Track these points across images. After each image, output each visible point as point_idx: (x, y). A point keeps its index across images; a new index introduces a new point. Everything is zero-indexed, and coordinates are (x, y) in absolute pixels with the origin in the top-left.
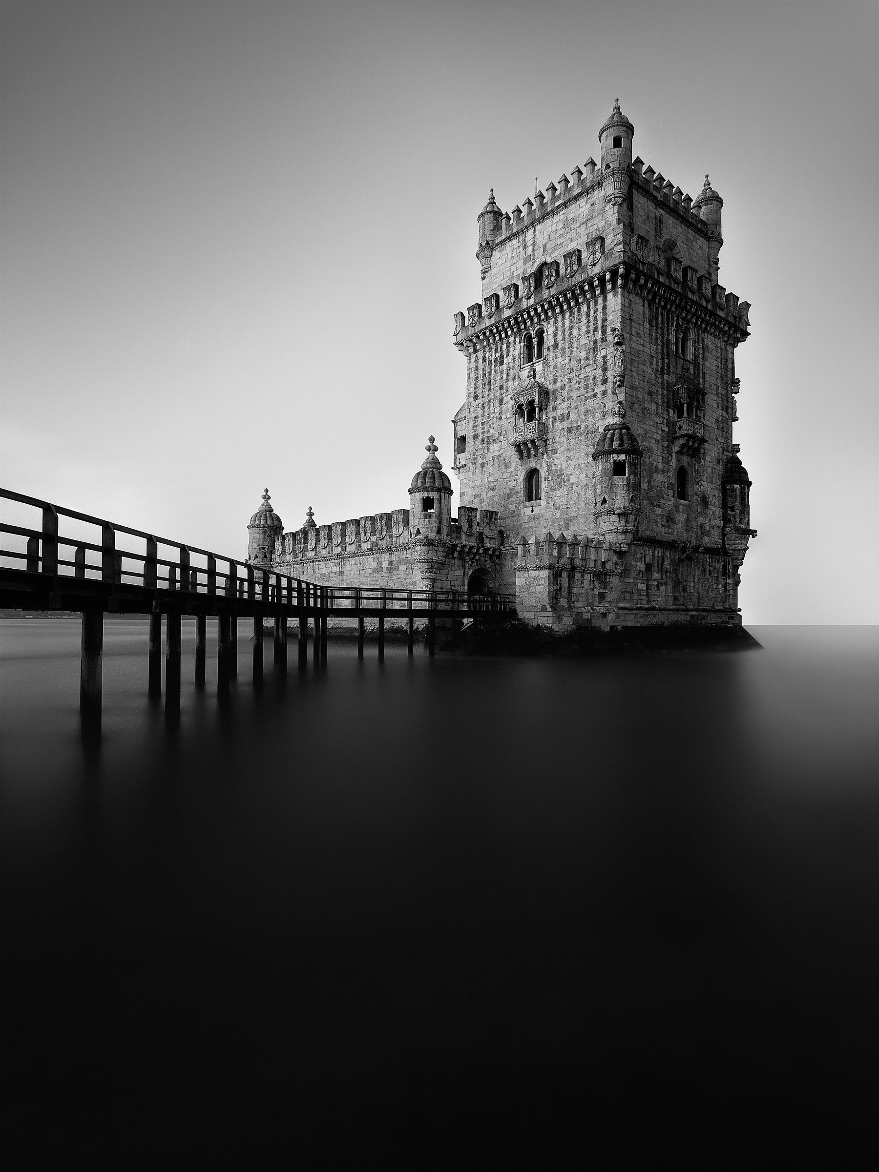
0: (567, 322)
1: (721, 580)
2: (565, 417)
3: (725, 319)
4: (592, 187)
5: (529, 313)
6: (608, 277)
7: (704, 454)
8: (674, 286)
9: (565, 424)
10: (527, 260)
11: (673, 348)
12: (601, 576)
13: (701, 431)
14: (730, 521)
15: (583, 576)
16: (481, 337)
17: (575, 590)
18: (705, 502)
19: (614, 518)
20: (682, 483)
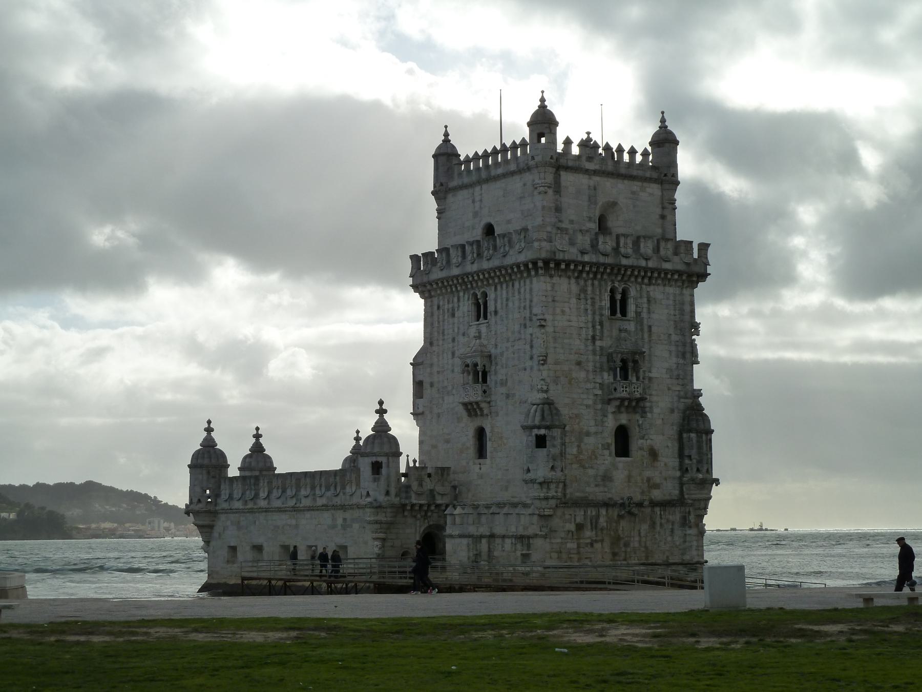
0: (504, 292)
1: (678, 532)
2: (504, 383)
3: (671, 271)
4: (523, 169)
5: (473, 277)
6: (530, 266)
7: (651, 407)
8: (602, 259)
9: (503, 390)
10: (476, 214)
11: (607, 312)
12: (523, 539)
13: (640, 390)
14: (687, 469)
15: (503, 541)
16: (435, 286)
17: (496, 554)
18: (653, 454)
19: (536, 486)
20: (622, 442)
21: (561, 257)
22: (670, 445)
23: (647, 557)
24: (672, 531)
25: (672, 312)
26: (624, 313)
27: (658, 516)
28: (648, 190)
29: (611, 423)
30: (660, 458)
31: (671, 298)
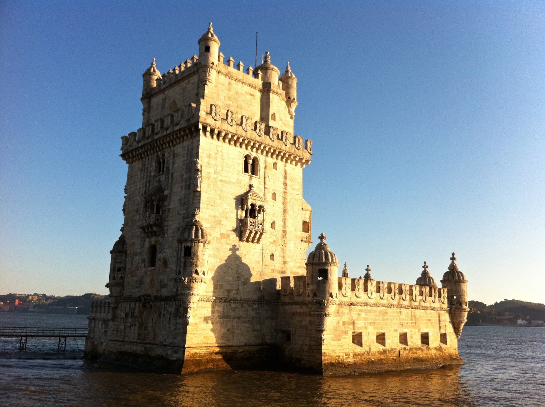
1: (172, 321)
7: (167, 230)
12: (105, 322)
17: (96, 329)
18: (165, 263)
21: (130, 149)
22: (175, 255)
23: (154, 338)
24: (170, 319)
25: (186, 158)
26: (163, 171)
27: (163, 310)
28: (192, 82)
29: (147, 245)
30: (168, 266)
31: (186, 149)
